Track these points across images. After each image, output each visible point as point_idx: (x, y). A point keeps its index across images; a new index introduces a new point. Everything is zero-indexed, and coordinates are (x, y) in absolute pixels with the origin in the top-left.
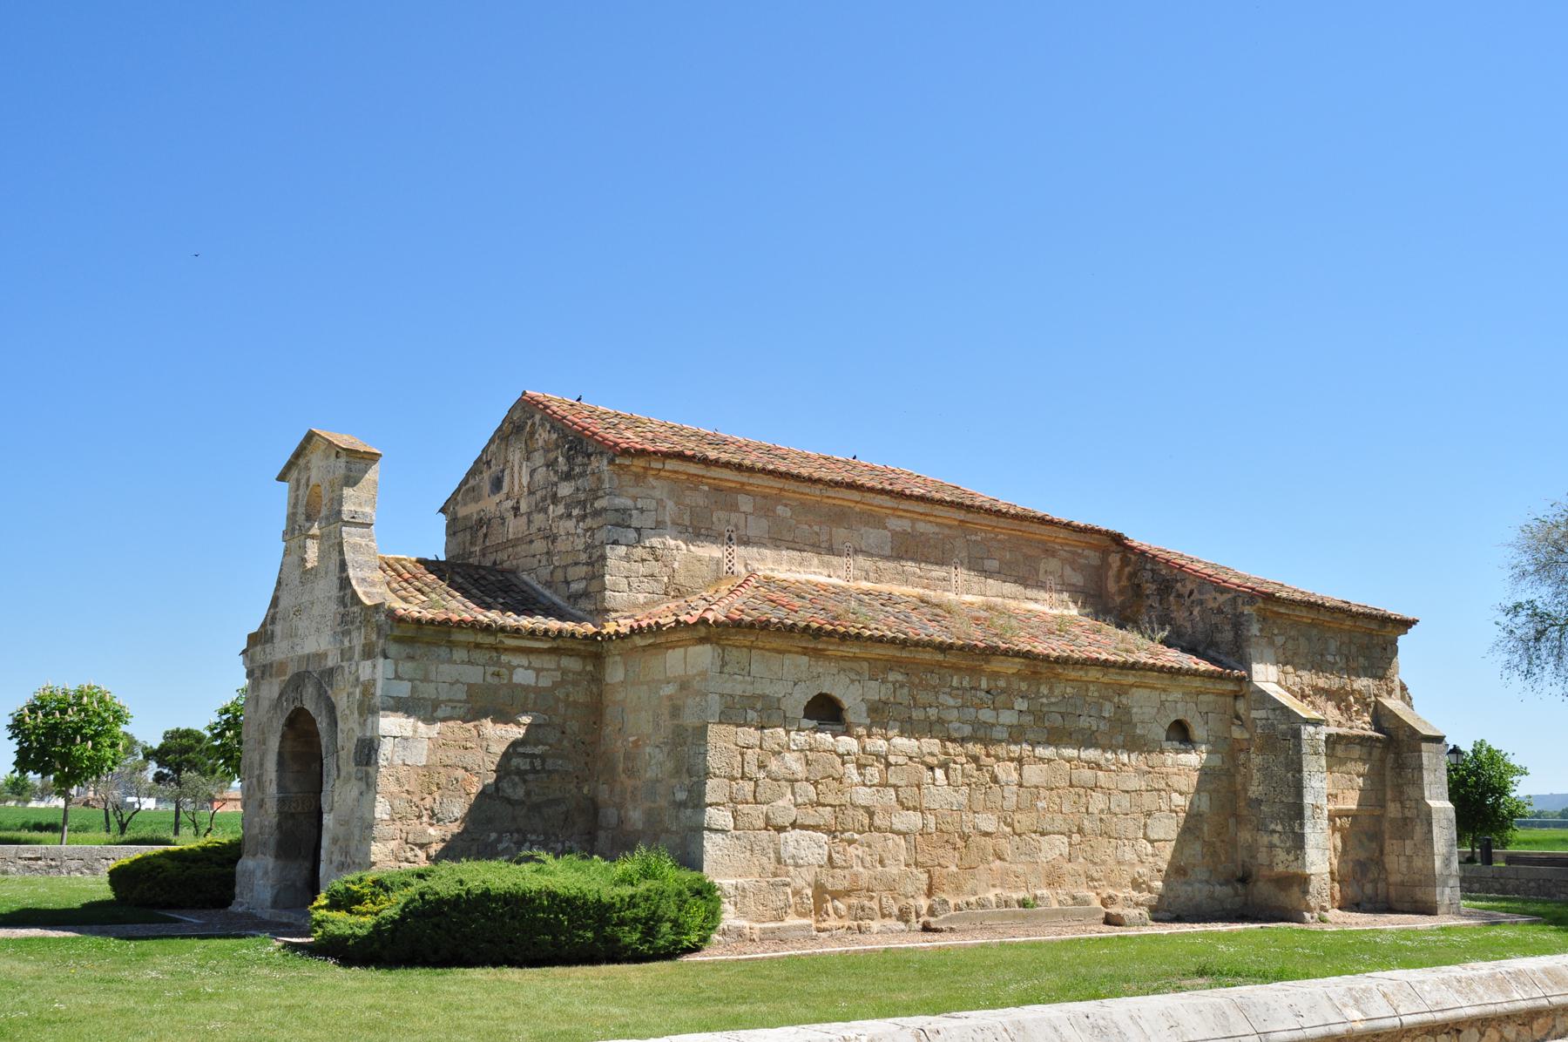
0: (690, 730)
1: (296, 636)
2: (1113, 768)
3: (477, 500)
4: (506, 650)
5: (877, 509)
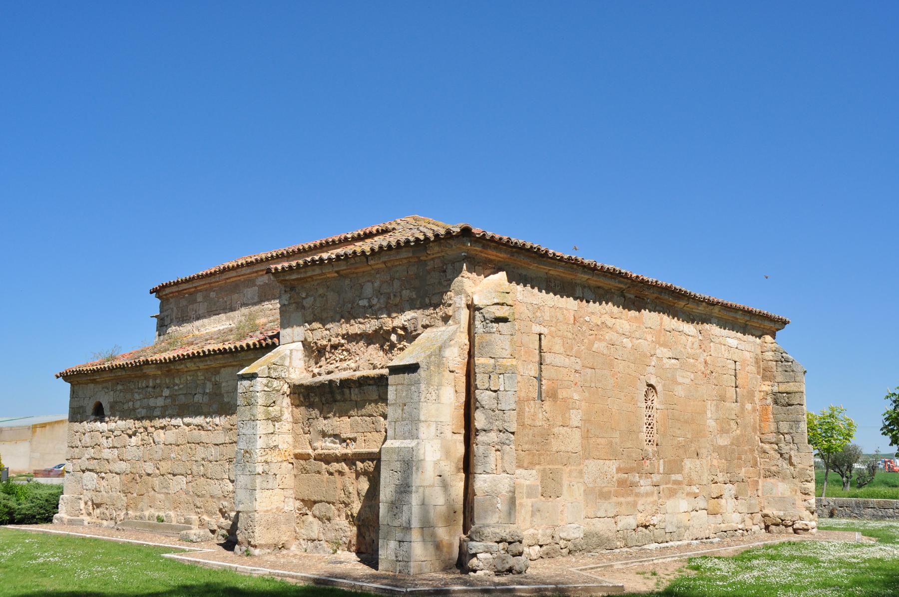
2: (210, 428)
5: (250, 276)
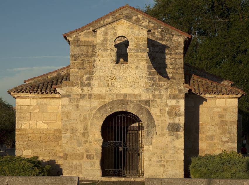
0: (229, 122)
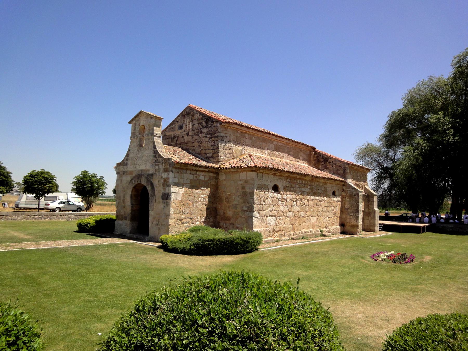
1: (137, 164)
3: (174, 131)
4: (198, 171)
